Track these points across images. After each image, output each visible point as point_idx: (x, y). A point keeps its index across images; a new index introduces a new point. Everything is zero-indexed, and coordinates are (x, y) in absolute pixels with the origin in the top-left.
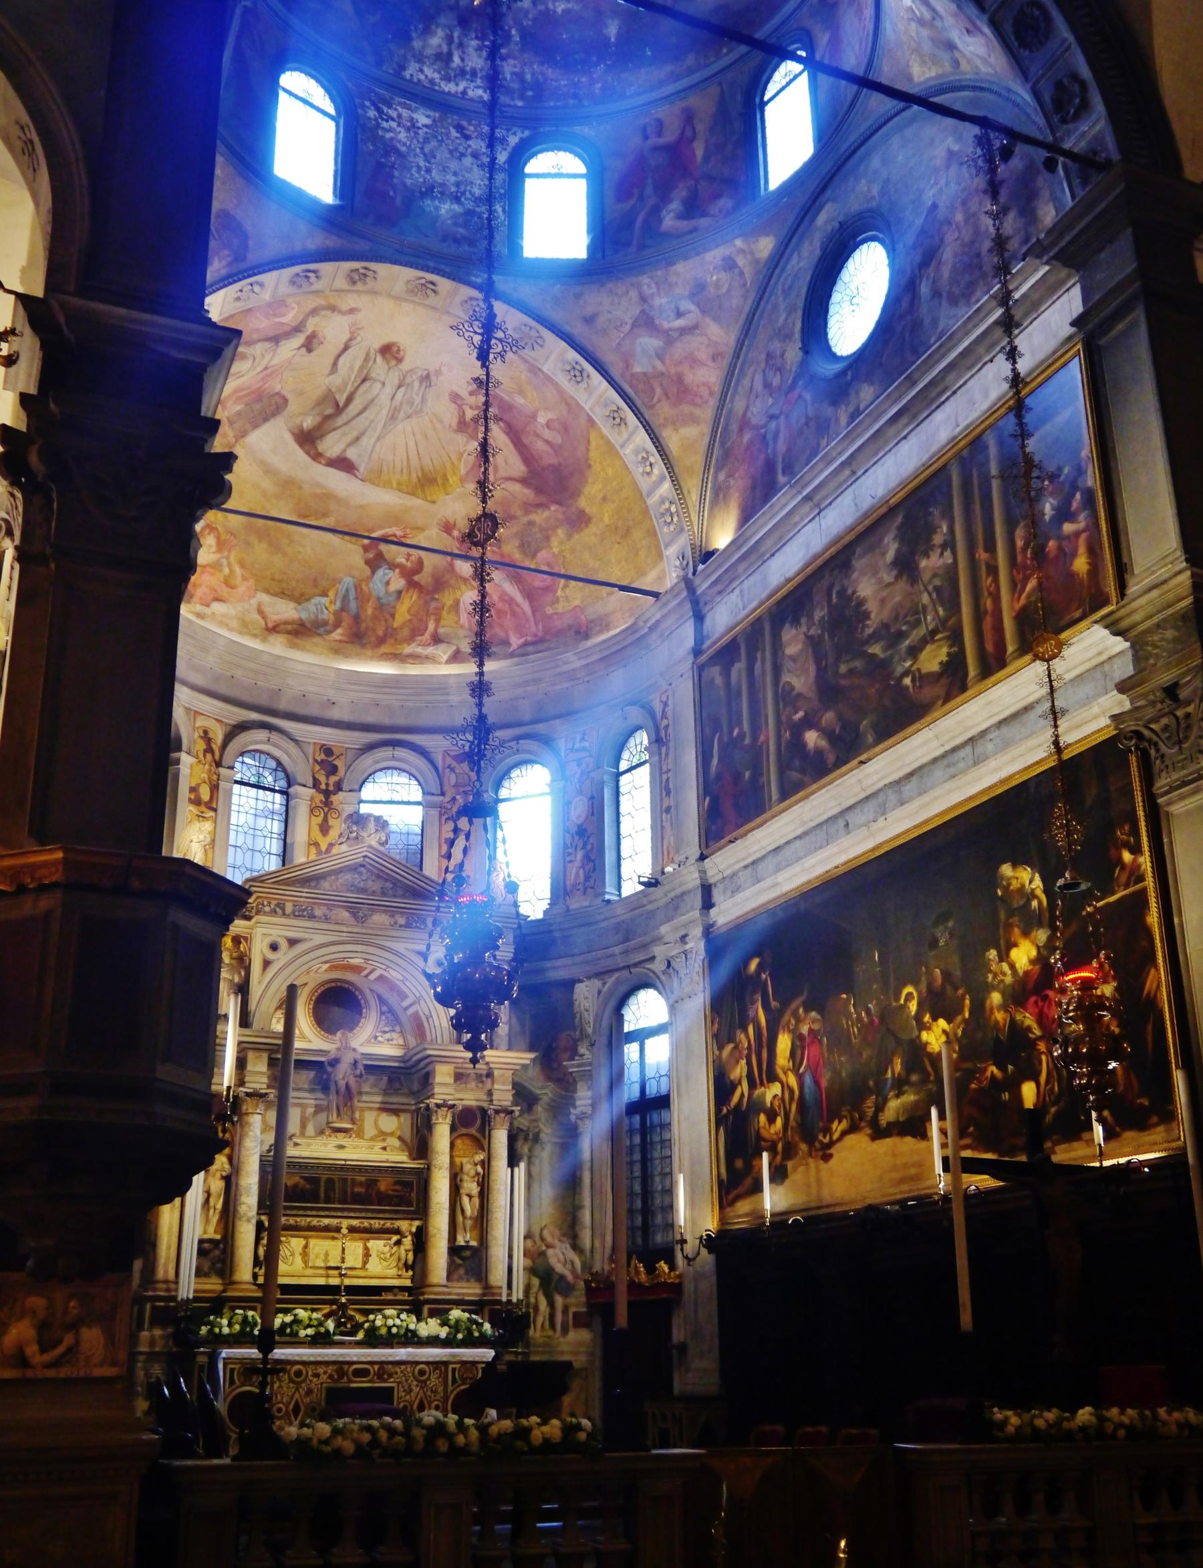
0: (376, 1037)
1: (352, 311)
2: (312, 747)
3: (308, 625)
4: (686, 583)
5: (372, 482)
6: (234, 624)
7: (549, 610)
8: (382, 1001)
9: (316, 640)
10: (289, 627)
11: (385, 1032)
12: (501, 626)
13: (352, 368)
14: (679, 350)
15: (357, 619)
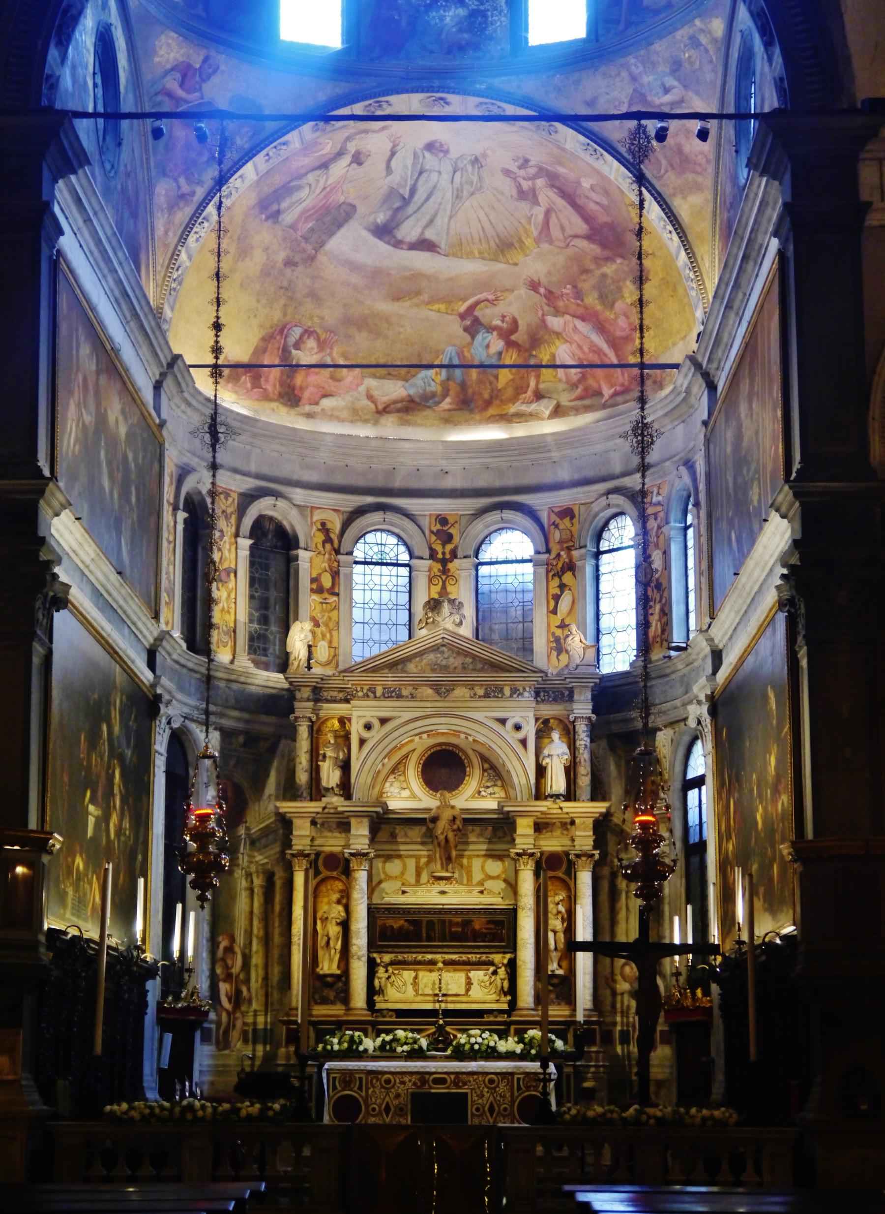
0: (479, 792)
3: (417, 400)
5: (455, 255)
6: (345, 414)
8: (484, 759)
9: (427, 412)
10: (399, 405)
11: (488, 787)
13: (405, 167)
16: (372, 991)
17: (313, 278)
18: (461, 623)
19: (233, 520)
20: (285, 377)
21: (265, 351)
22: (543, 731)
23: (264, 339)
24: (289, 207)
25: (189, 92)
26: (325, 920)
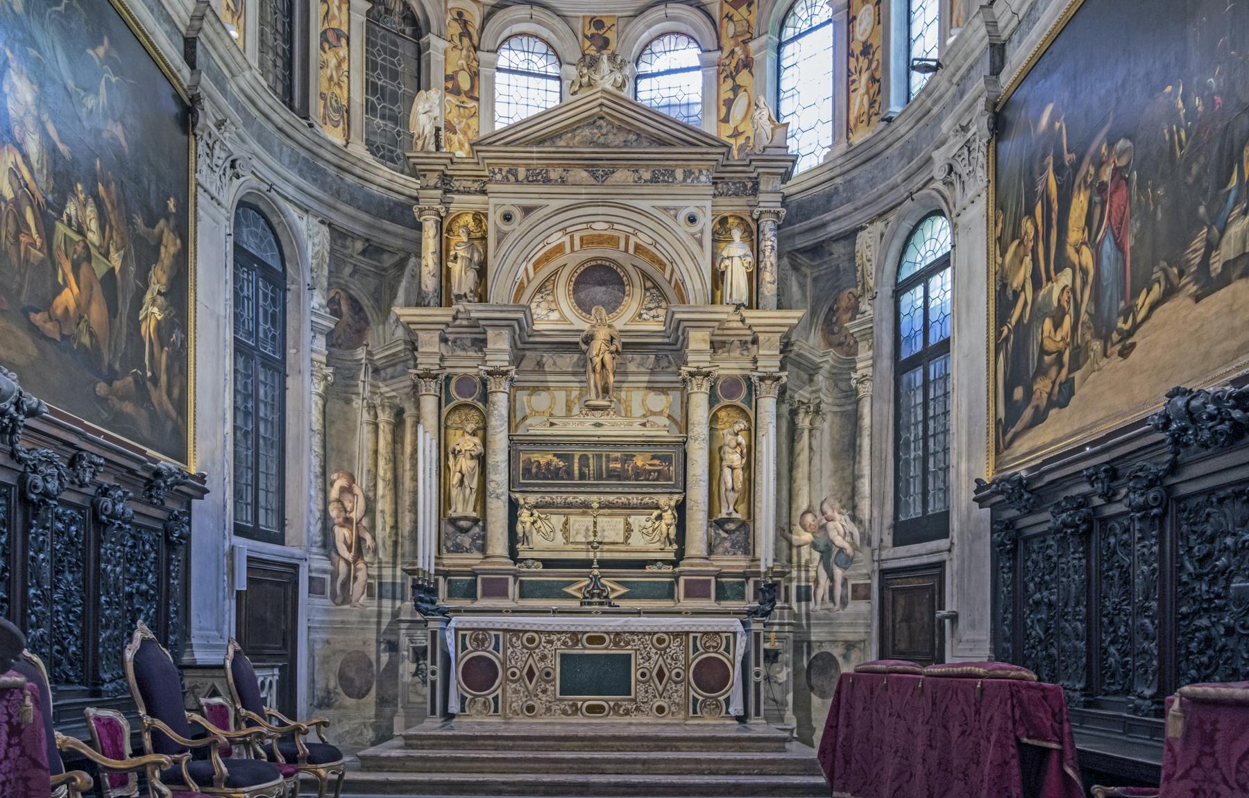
16: (513, 538)
18: (623, 85)
22: (721, 234)
26: (456, 454)
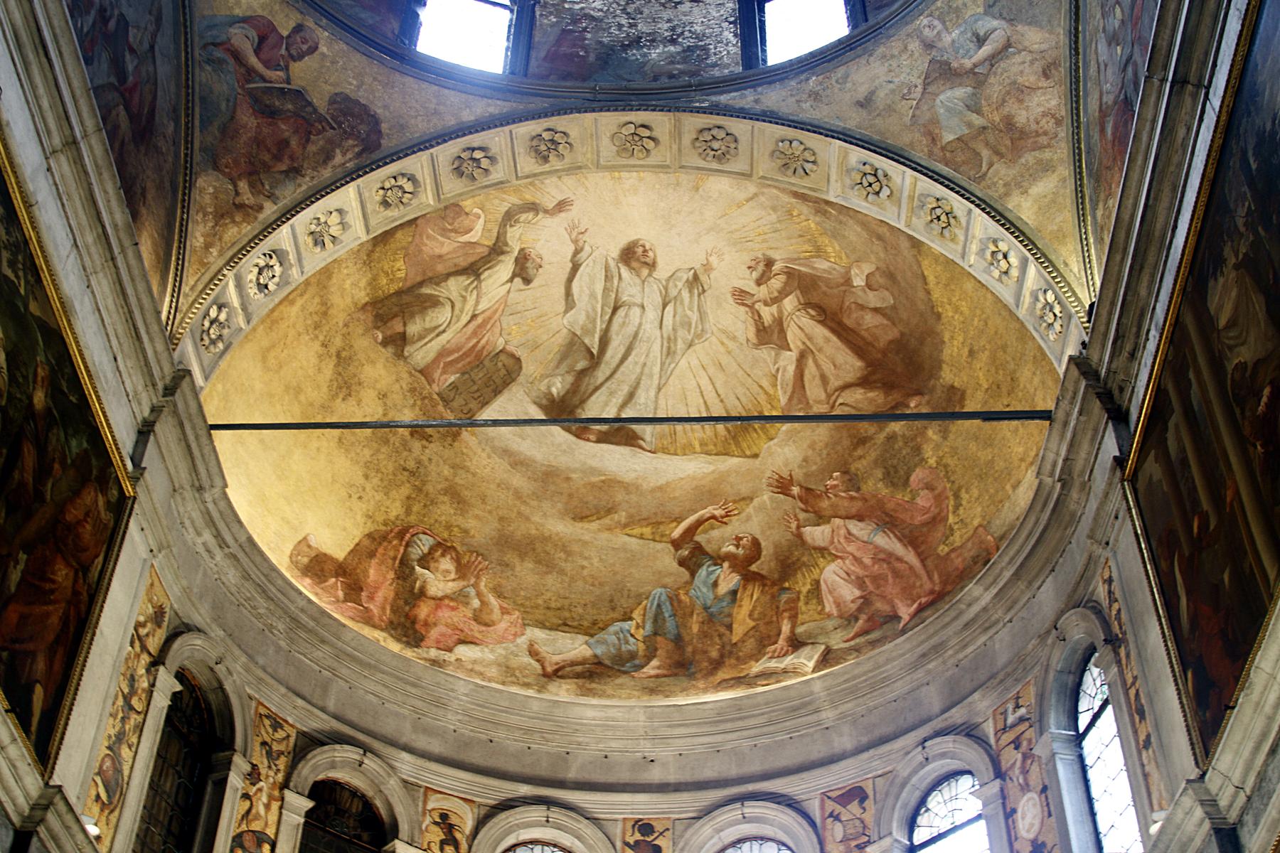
1: (561, 206)
2: (620, 825)
3: (607, 662)
4: (1077, 365)
5: (665, 451)
6: (493, 672)
7: (943, 550)
10: (579, 669)
12: (883, 597)
13: (593, 295)
14: (995, 87)
15: (678, 640)
17: (454, 467)
19: (282, 763)
20: (401, 603)
21: (372, 555)
23: (369, 536)
24: (421, 338)
25: (267, 64)
